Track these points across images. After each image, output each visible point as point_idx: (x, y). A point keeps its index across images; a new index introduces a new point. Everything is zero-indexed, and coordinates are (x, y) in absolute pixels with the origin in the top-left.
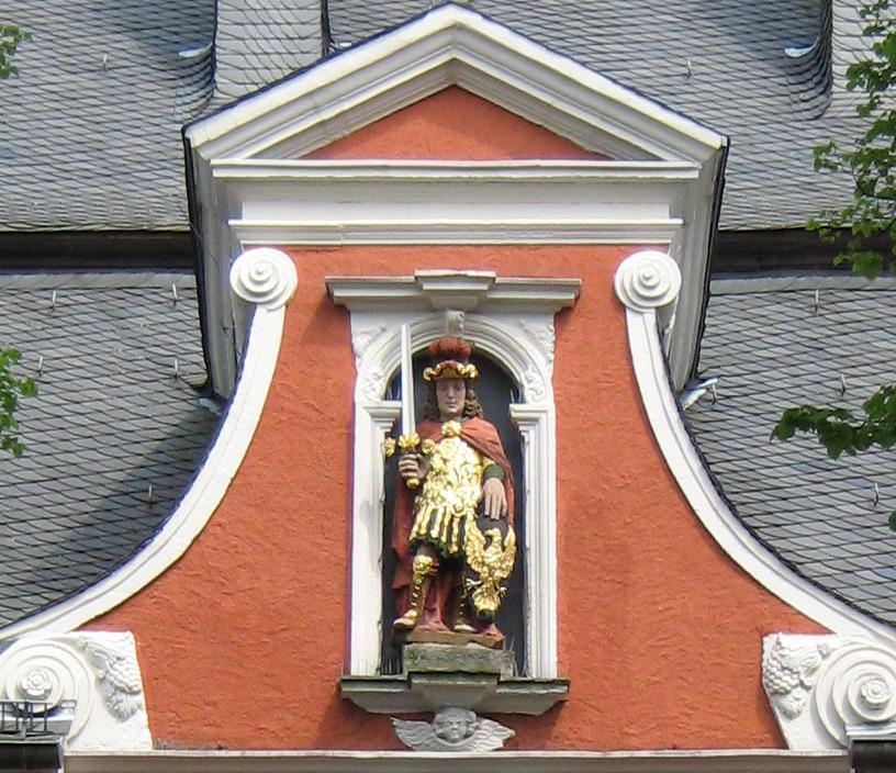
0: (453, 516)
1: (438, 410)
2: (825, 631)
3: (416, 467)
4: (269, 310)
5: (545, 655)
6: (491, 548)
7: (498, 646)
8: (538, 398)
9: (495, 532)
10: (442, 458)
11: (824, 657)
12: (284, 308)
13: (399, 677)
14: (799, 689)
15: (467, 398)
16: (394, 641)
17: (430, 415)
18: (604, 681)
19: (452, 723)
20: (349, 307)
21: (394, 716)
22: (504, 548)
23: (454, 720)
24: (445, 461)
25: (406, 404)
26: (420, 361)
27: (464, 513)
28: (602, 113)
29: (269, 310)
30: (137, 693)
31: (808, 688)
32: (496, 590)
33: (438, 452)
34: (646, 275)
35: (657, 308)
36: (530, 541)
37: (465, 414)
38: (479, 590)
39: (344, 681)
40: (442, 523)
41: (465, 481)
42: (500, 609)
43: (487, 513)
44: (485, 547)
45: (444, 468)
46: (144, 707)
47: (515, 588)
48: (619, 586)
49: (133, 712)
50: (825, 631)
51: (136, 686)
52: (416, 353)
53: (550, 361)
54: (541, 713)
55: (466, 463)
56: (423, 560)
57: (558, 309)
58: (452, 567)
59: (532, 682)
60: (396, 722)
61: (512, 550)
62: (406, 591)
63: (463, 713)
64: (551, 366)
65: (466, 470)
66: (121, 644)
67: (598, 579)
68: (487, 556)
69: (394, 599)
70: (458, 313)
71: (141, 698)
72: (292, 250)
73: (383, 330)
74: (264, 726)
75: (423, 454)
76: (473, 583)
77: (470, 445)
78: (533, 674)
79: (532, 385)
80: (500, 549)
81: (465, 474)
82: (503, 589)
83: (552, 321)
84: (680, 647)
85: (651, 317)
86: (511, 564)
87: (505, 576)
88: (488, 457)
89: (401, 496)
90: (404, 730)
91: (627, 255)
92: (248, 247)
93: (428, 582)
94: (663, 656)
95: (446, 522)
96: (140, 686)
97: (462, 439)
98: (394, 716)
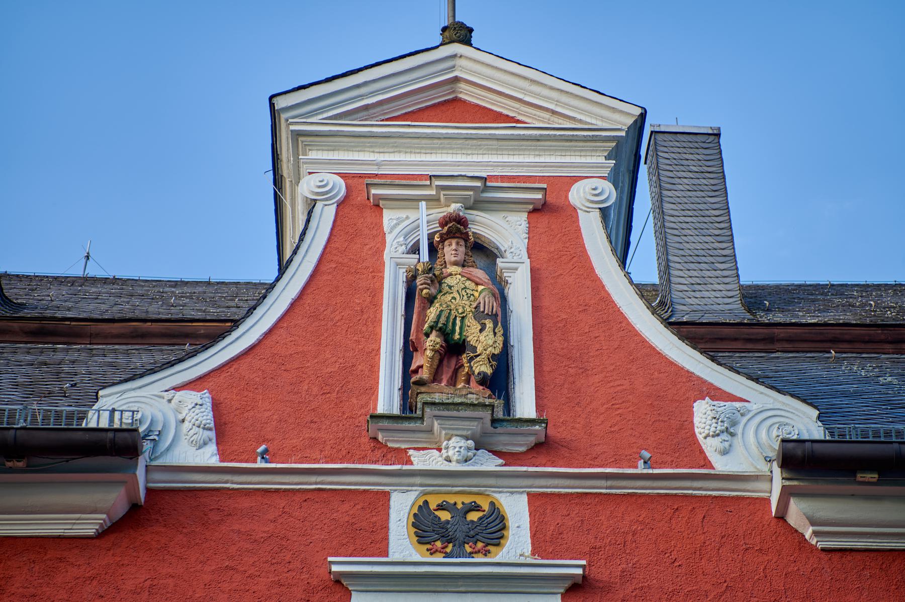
0: (456, 316)
1: (445, 262)
3: (429, 282)
4: (326, 205)
6: (484, 332)
7: (490, 397)
9: (489, 324)
10: (448, 285)
11: (742, 415)
12: (336, 204)
13: (414, 415)
14: (725, 434)
15: (465, 254)
18: (573, 430)
19: (455, 447)
20: (381, 203)
21: (409, 449)
22: (495, 334)
24: (450, 287)
27: (465, 315)
28: (557, 101)
29: (326, 205)
30: (210, 429)
31: (732, 435)
32: (490, 362)
33: (445, 283)
34: (594, 187)
35: (600, 209)
36: (513, 341)
38: (478, 359)
39: (372, 417)
40: (448, 318)
41: (465, 297)
42: (494, 374)
43: (482, 309)
44: (481, 331)
45: (449, 290)
46: (214, 440)
48: (581, 371)
49: (205, 444)
51: (210, 424)
52: (430, 233)
53: (526, 238)
54: (522, 449)
55: (465, 288)
57: (531, 207)
59: (520, 421)
60: (411, 452)
61: (500, 339)
62: (420, 370)
63: (463, 441)
64: (527, 240)
65: (465, 291)
67: (565, 366)
70: (459, 205)
71: (212, 434)
73: (407, 218)
74: (309, 455)
75: (434, 275)
76: (472, 355)
77: (469, 279)
78: (518, 415)
79: (512, 250)
80: (492, 333)
81: (464, 294)
82: (494, 363)
83: (527, 216)
84: (629, 410)
85: (596, 215)
86: (500, 347)
87: (496, 353)
88: (482, 285)
91: (576, 181)
92: (310, 173)
93: (437, 357)
94: (618, 415)
95: (452, 317)
96: (212, 425)
97: (463, 276)
98: (409, 449)
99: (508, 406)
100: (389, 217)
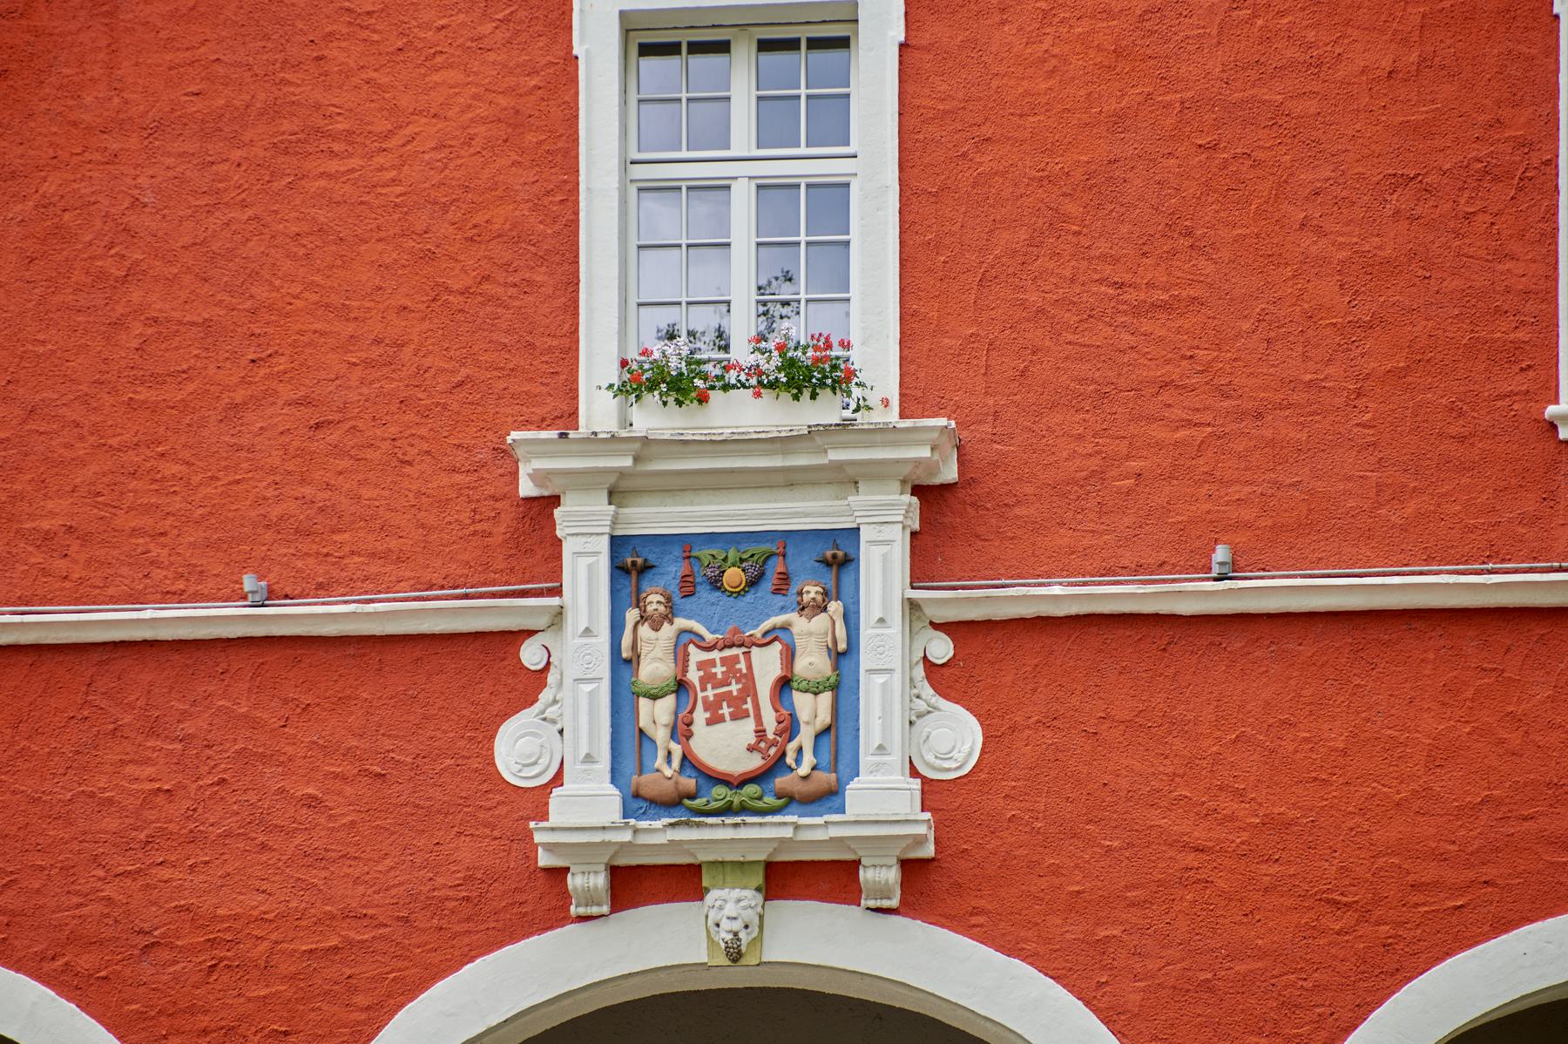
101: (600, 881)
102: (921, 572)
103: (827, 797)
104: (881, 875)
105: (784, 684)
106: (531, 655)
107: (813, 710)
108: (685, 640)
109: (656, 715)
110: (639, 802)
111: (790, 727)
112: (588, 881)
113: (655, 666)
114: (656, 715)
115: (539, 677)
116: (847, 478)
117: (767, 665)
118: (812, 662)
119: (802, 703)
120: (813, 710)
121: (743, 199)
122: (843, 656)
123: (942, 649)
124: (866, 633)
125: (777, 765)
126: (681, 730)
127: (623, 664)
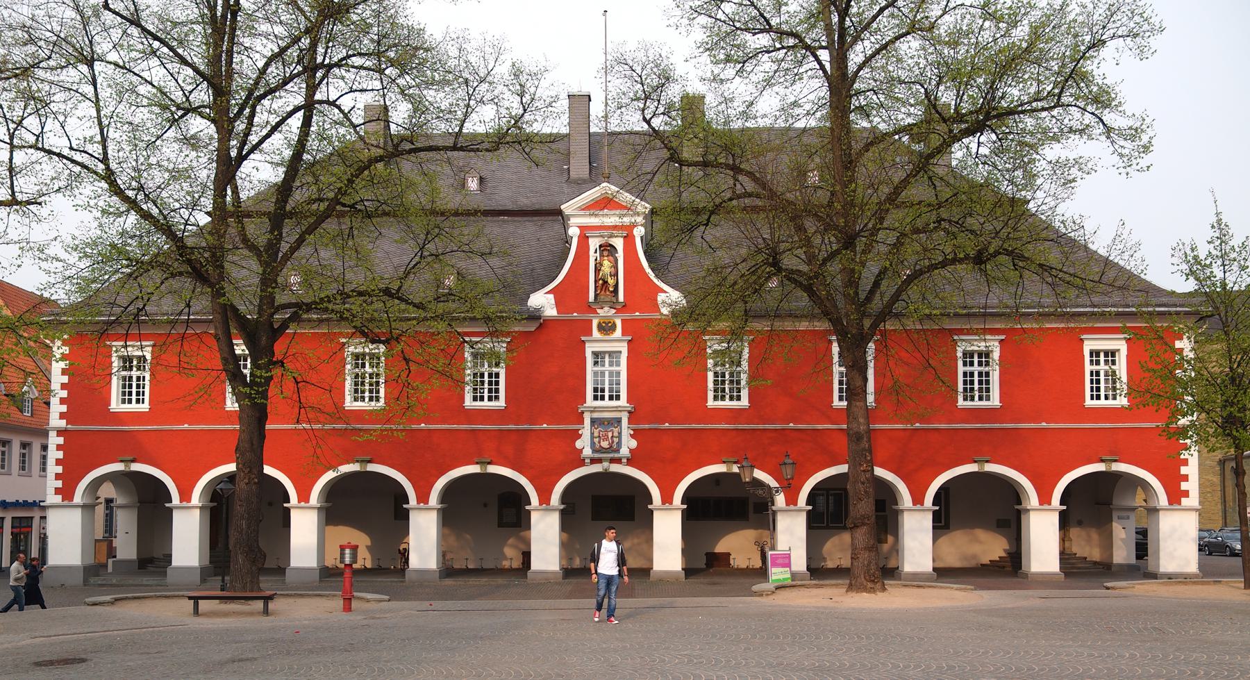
2: (665, 292)
5: (621, 298)
8: (620, 255)
16: (596, 296)
17: (601, 255)
23: (606, 309)
25: (598, 254)
26: (600, 246)
37: (608, 256)
47: (616, 286)
50: (665, 292)
56: (601, 282)
58: (605, 282)
66: (551, 296)
68: (611, 281)
69: (596, 287)
72: (579, 227)
89: (597, 270)
90: (599, 311)
99: (617, 299)
100: (591, 240)
101: (589, 461)
102: (630, 422)
103: (618, 451)
104: (624, 461)
105: (612, 437)
106: (580, 432)
107: (616, 440)
108: (600, 431)
109: (596, 440)
110: (594, 451)
111: (613, 442)
112: (587, 461)
113: (596, 434)
114: (596, 440)
115: (581, 435)
116: (620, 411)
117: (610, 435)
118: (616, 434)
119: (615, 439)
120: (616, 440)
121: (607, 374)
122: (620, 433)
123: (632, 432)
124: (623, 431)
125: (611, 447)
126: (599, 442)
127: (592, 434)
